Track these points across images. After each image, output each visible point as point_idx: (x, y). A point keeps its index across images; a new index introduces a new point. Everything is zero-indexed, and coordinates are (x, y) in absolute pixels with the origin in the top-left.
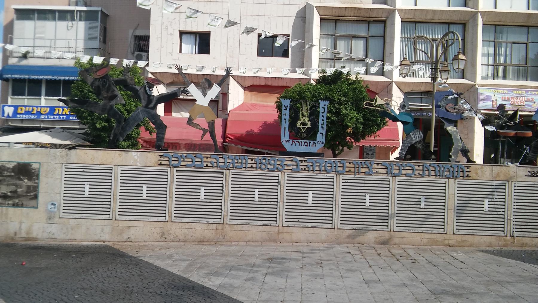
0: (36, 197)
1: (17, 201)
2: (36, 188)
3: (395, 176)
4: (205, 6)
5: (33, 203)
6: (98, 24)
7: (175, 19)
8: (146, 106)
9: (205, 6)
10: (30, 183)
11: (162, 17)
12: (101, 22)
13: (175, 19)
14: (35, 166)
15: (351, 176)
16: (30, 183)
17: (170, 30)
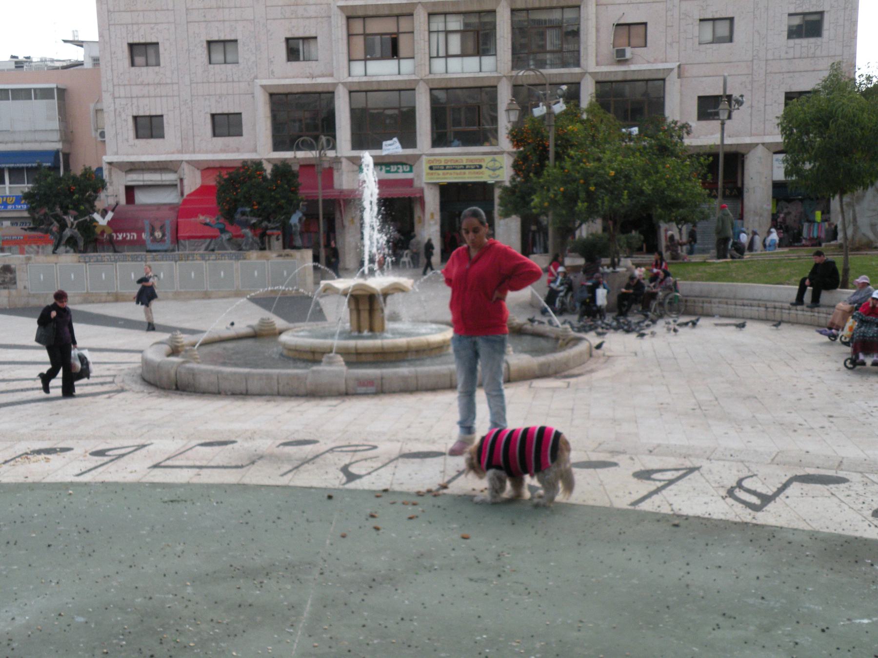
0: (15, 283)
1: (5, 286)
2: (15, 278)
3: (206, 260)
4: (155, 89)
5: (14, 286)
6: (55, 102)
7: (127, 104)
8: (71, 227)
9: (155, 89)
10: (11, 276)
11: (115, 103)
12: (58, 99)
13: (127, 104)
14: (13, 266)
15: (183, 262)
16: (11, 276)
17: (124, 116)
